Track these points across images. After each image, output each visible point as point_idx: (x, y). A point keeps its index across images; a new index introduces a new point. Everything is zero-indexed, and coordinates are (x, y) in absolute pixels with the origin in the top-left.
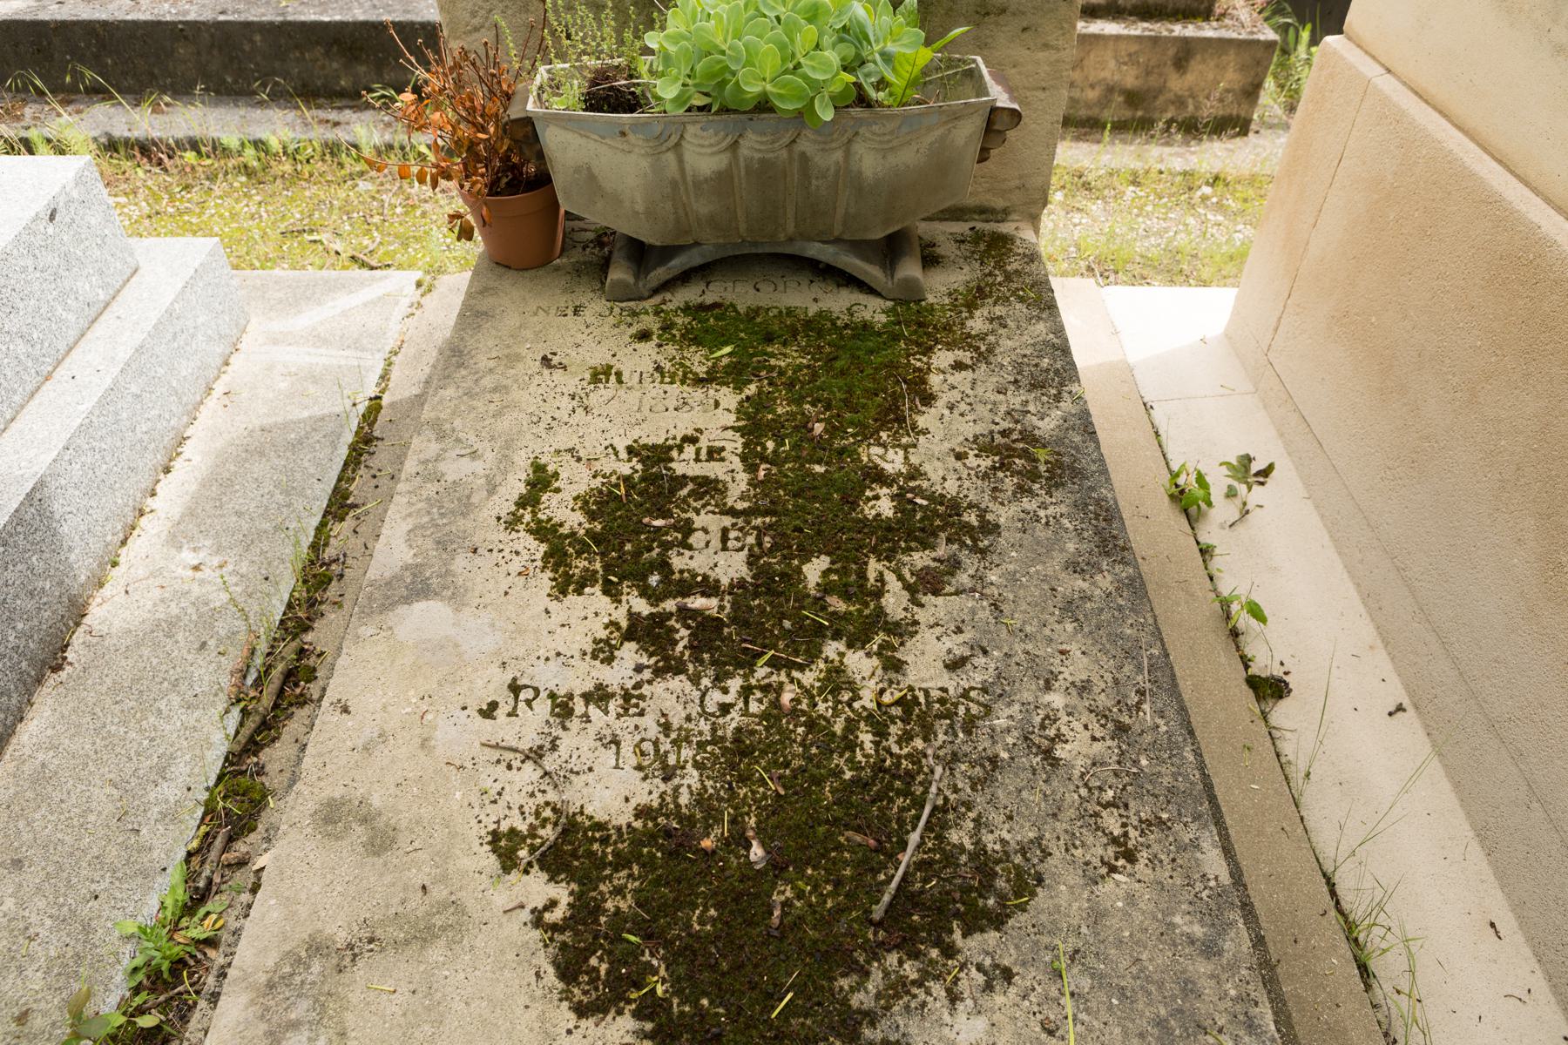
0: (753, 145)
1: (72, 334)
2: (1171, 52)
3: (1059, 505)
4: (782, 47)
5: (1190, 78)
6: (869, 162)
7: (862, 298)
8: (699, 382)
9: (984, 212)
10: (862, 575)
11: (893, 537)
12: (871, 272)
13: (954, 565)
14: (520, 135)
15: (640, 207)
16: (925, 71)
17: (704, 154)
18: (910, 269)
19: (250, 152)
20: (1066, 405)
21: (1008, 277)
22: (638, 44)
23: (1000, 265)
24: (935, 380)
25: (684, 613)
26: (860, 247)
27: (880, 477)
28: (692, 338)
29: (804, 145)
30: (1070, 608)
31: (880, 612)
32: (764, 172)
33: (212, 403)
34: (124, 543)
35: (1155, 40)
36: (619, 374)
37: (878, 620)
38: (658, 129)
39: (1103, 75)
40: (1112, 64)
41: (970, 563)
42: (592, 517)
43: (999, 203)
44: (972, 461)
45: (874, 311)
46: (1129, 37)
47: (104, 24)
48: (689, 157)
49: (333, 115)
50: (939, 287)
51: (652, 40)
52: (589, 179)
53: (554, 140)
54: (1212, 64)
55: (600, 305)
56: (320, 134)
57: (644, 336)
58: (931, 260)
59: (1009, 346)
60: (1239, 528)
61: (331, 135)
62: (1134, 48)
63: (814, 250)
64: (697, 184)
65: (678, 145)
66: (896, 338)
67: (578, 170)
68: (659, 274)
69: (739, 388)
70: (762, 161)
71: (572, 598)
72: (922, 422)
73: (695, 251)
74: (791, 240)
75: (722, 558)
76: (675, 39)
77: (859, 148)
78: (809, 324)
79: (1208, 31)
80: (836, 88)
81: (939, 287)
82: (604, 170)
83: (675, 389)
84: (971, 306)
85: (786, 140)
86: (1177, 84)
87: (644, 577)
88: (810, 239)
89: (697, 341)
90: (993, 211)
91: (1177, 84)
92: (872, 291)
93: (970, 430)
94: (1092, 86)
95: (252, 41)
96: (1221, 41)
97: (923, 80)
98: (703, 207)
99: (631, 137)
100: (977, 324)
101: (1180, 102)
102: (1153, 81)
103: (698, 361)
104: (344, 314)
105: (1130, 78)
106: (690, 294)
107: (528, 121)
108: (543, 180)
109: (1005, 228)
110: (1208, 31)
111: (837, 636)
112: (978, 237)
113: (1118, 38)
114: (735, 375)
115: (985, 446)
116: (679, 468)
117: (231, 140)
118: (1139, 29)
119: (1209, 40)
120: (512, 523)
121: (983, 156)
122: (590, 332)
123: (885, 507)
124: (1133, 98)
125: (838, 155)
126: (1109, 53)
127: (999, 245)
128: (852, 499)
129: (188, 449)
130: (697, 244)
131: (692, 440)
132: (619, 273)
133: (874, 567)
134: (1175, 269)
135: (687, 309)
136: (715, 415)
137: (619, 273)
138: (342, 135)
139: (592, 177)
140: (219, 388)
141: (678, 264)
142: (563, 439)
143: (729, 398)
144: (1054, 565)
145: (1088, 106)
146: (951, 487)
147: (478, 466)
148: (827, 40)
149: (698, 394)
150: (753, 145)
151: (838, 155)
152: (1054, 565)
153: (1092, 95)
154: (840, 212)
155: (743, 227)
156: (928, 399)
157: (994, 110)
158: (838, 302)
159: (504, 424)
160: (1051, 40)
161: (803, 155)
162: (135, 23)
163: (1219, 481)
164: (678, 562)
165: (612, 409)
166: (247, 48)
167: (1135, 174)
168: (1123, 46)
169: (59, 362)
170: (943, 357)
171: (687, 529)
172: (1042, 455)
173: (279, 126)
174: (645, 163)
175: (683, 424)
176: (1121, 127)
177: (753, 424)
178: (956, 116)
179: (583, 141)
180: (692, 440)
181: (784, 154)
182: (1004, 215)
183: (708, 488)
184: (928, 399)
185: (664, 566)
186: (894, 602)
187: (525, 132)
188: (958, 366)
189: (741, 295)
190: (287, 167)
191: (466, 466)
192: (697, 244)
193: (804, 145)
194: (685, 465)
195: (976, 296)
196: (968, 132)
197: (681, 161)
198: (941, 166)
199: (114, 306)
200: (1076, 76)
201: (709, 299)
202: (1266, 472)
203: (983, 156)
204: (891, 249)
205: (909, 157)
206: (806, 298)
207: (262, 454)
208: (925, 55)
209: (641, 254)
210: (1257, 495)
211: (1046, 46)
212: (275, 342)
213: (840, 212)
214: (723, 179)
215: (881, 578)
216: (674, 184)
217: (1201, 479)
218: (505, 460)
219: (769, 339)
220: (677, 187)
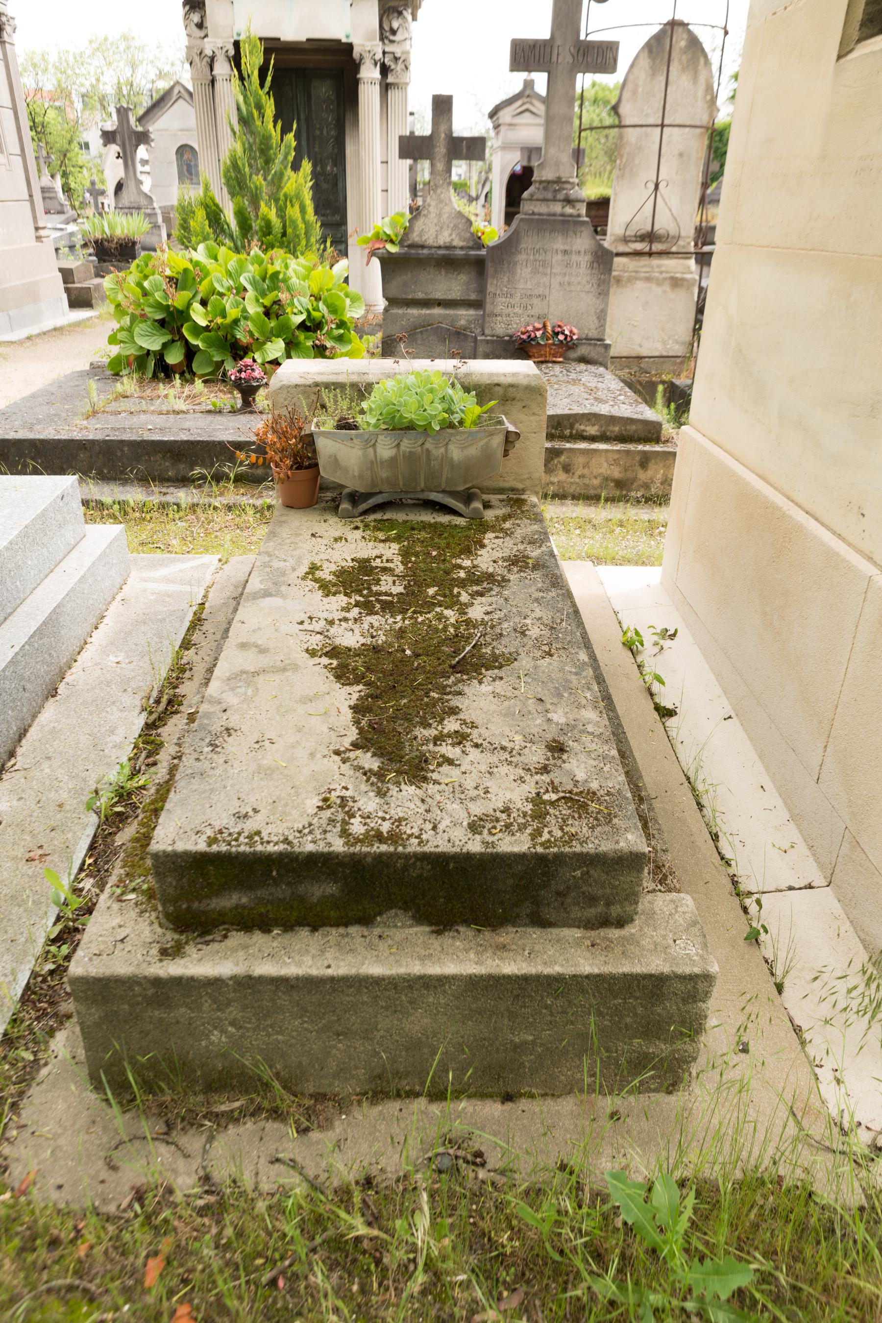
0: (407, 444)
1: (62, 555)
2: (638, 458)
3: (537, 575)
4: (419, 402)
5: (650, 473)
6: (456, 453)
7: (455, 518)
8: (383, 541)
9: (513, 490)
10: (451, 591)
11: (463, 584)
12: (458, 506)
13: (491, 589)
14: (307, 441)
15: (356, 474)
16: (479, 417)
17: (385, 450)
18: (477, 505)
19: (116, 507)
20: (544, 548)
21: (523, 512)
22: (358, 409)
23: (519, 508)
24: (486, 542)
25: (378, 601)
26: (453, 494)
27: (460, 567)
28: (377, 529)
29: (429, 445)
30: (537, 600)
31: (458, 601)
32: (411, 457)
33: (115, 603)
34: (79, 653)
35: (628, 452)
36: (346, 540)
37: (458, 602)
38: (366, 437)
39: (601, 471)
40: (605, 465)
41: (496, 589)
42: (338, 577)
43: (520, 486)
44: (500, 563)
45: (460, 521)
46: (613, 451)
47: (42, 441)
48: (379, 450)
49: (164, 490)
50: (489, 515)
51: (365, 405)
52: (335, 461)
53: (322, 444)
54: (661, 465)
55: (336, 519)
56: (156, 499)
57: (357, 528)
58: (487, 505)
59: (519, 533)
60: (659, 657)
61: (164, 499)
62: (616, 456)
63: (434, 496)
64: (382, 463)
65: (374, 445)
66: (470, 529)
67: (330, 457)
68: (363, 506)
69: (399, 543)
70: (410, 452)
71: (331, 597)
72: (479, 553)
73: (380, 496)
74: (423, 491)
75: (393, 588)
76: (374, 402)
77: (451, 447)
78: (430, 525)
79: (657, 448)
80: (440, 418)
81: (489, 515)
82: (342, 458)
83: (372, 543)
84: (504, 520)
85: (420, 443)
86: (643, 476)
87: (361, 591)
88: (431, 491)
89: (380, 529)
90: (517, 490)
91: (643, 476)
92: (461, 515)
93: (500, 555)
94: (596, 477)
95: (122, 451)
96: (664, 452)
97: (478, 421)
98: (384, 474)
99: (355, 441)
100: (507, 525)
101: (646, 486)
102: (630, 474)
103: (381, 535)
104: (181, 571)
105: (617, 473)
106: (378, 516)
107: (311, 435)
108: (314, 466)
109: (523, 497)
110: (657, 448)
111: (440, 606)
112: (509, 499)
113: (607, 451)
114: (398, 539)
115: (504, 560)
116: (374, 564)
117: (107, 500)
118: (619, 447)
119: (658, 452)
120: (304, 578)
121: (506, 453)
122: (333, 527)
123: (462, 574)
124: (620, 484)
125: (442, 450)
126: (603, 460)
127: (520, 502)
128: (447, 573)
129: (106, 620)
130: (381, 492)
131: (380, 557)
132: (345, 506)
133: (456, 590)
134: (641, 561)
135: (375, 520)
136: (391, 551)
137: (345, 506)
138: (169, 499)
139: (336, 460)
140: (119, 598)
141: (372, 502)
142: (324, 557)
143: (395, 546)
144: (533, 589)
145: (594, 488)
146: (491, 570)
147: (287, 564)
148: (436, 400)
149: (382, 545)
150: (407, 444)
151: (442, 450)
152: (533, 589)
153: (596, 482)
154: (444, 477)
155: (401, 484)
156: (483, 546)
157: (508, 432)
158: (444, 519)
159: (298, 552)
160: (536, 411)
161: (428, 450)
162: (59, 440)
163: (649, 639)
164: (374, 588)
165: (344, 549)
166: (119, 454)
167: (621, 521)
168: (610, 455)
169: (56, 566)
170: (490, 535)
171: (380, 580)
172: (530, 561)
173: (134, 495)
174: (360, 453)
175: (375, 553)
176: (610, 500)
177: (405, 554)
178: (491, 434)
179: (334, 443)
180: (380, 557)
181: (419, 449)
182: (523, 491)
183: (385, 570)
184: (483, 546)
185: (369, 588)
186: (464, 598)
187: (309, 441)
188: (497, 537)
189: (400, 516)
190: (137, 514)
191: (282, 564)
192: (381, 492)
193: (429, 445)
194: (377, 563)
195: (505, 518)
196: (497, 441)
197: (375, 452)
198: (487, 457)
199: (77, 548)
200: (586, 471)
201: (385, 517)
202: (674, 635)
203: (506, 453)
204: (468, 497)
205: (473, 451)
206: (428, 517)
207: (145, 623)
208: (478, 410)
209: (355, 498)
210: (667, 643)
211: (534, 414)
212: (145, 581)
213: (444, 477)
214: (393, 460)
215: (459, 593)
216: (372, 462)
217: (637, 633)
218: (299, 560)
219: (413, 529)
220: (372, 464)
